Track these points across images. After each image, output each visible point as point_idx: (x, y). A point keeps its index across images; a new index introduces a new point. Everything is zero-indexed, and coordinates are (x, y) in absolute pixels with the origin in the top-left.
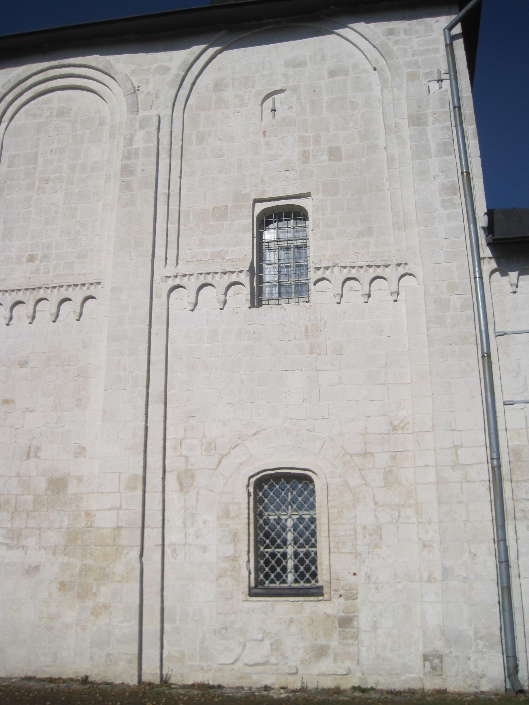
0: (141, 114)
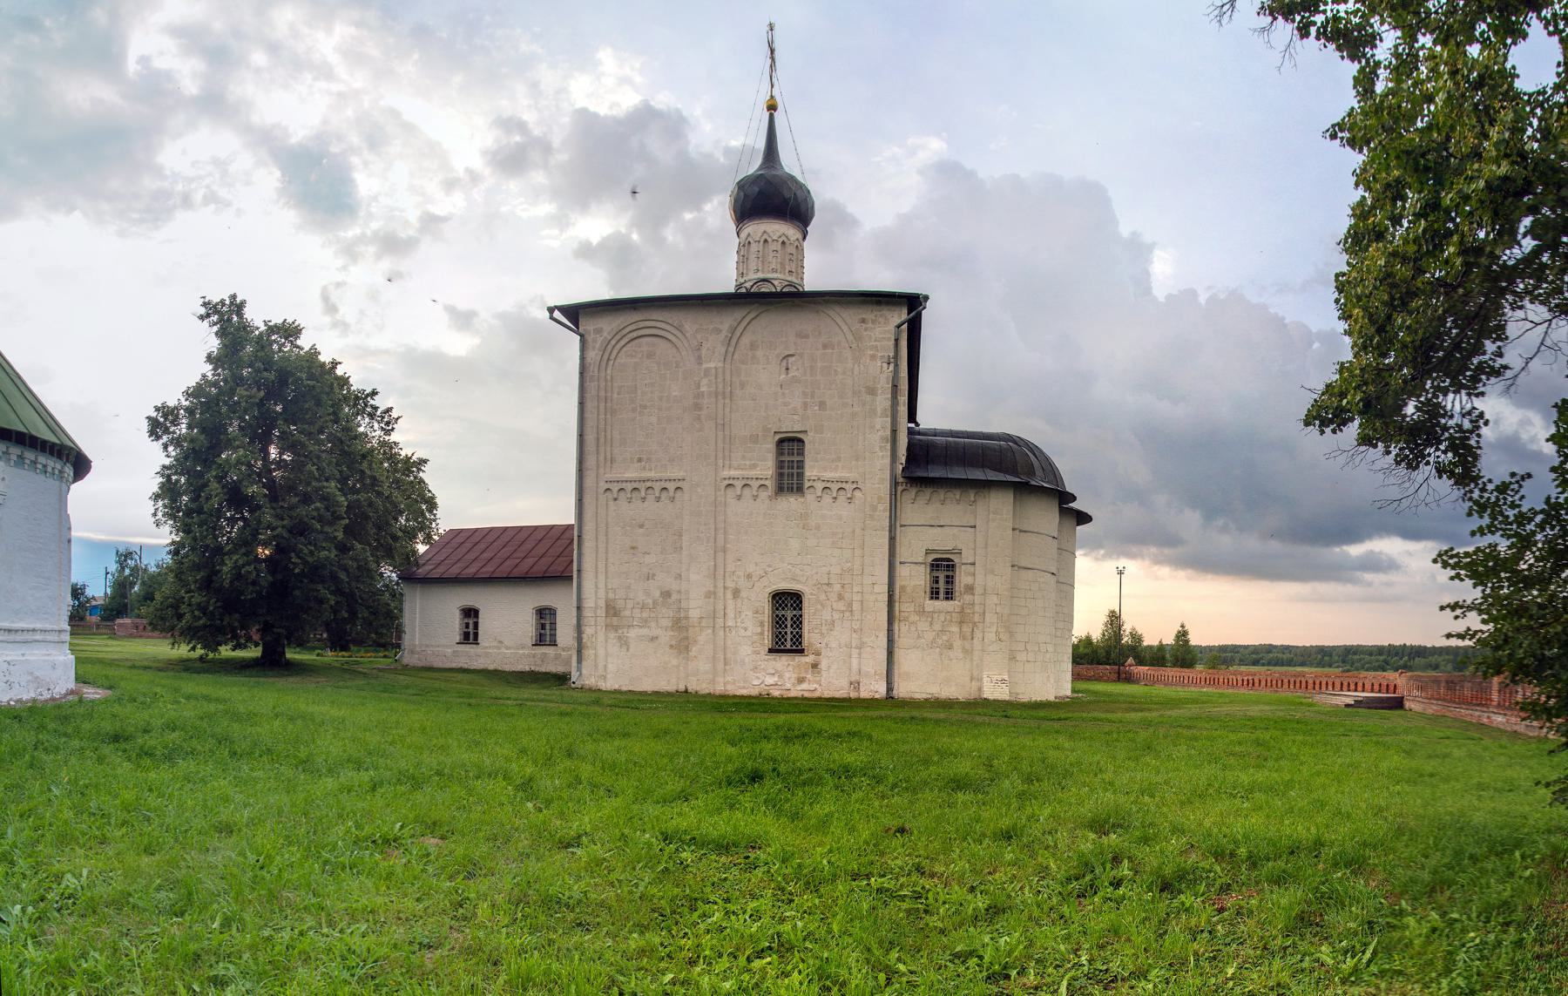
0: (704, 366)
